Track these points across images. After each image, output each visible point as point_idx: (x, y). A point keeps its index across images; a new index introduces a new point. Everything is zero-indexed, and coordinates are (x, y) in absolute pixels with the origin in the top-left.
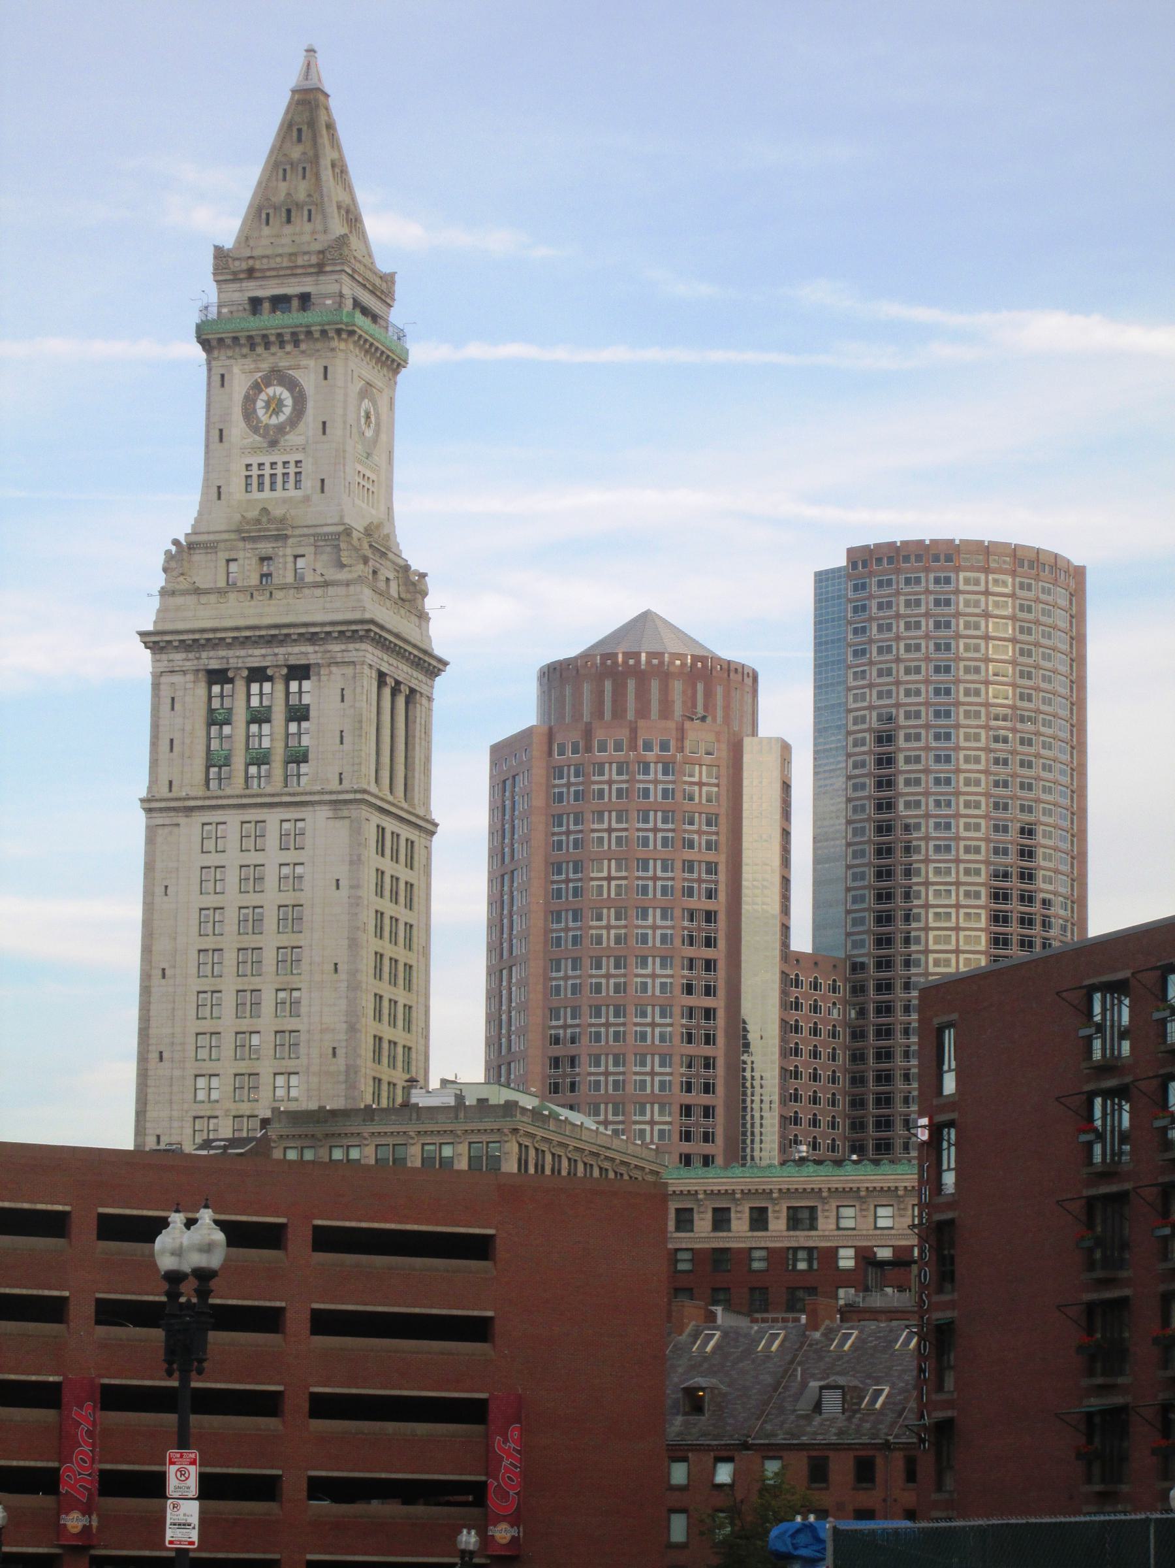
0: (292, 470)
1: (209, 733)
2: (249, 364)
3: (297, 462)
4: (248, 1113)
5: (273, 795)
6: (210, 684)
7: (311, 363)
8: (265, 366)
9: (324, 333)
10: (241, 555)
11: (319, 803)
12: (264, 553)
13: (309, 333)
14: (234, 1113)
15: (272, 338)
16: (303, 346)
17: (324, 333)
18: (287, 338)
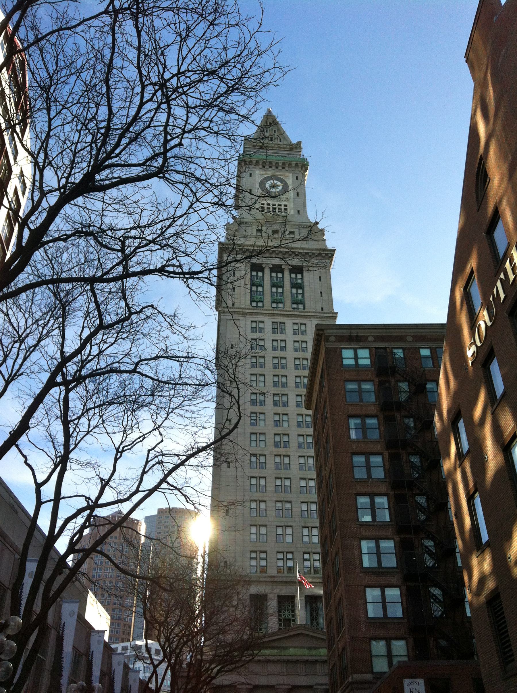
0: (283, 207)
1: (251, 288)
2: (262, 172)
3: (285, 206)
4: (284, 454)
5: (288, 311)
6: (252, 270)
7: (291, 175)
8: (270, 173)
9: (297, 165)
10: (264, 229)
11: (314, 317)
12: (275, 229)
13: (290, 164)
14: (275, 453)
15: (274, 164)
16: (287, 168)
17: (297, 165)
18: (280, 164)
